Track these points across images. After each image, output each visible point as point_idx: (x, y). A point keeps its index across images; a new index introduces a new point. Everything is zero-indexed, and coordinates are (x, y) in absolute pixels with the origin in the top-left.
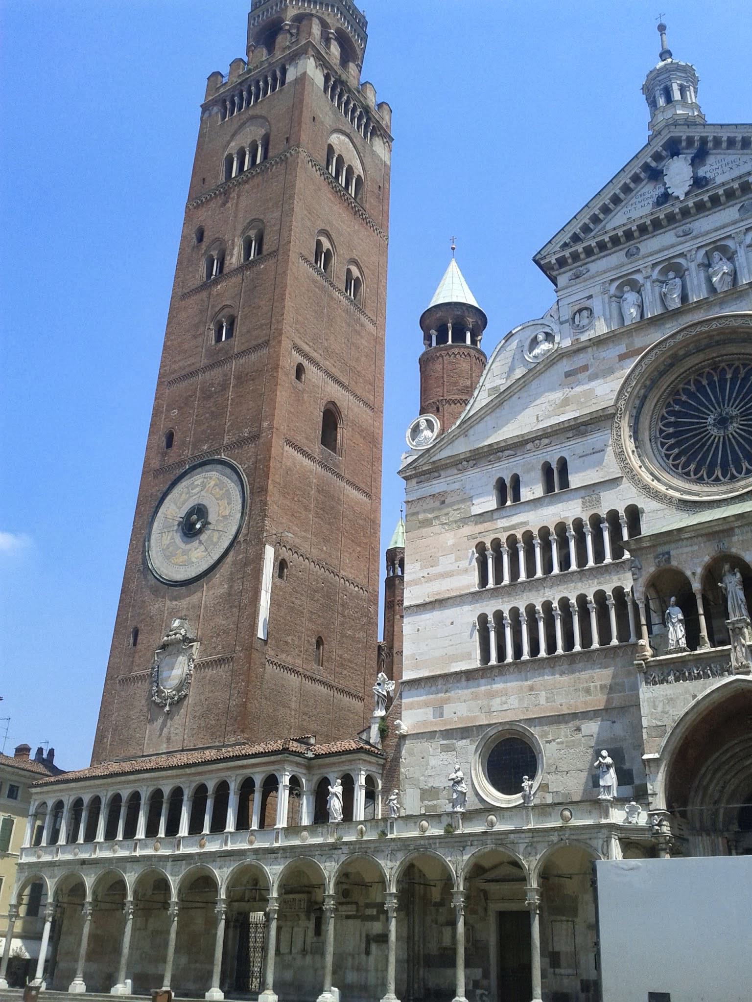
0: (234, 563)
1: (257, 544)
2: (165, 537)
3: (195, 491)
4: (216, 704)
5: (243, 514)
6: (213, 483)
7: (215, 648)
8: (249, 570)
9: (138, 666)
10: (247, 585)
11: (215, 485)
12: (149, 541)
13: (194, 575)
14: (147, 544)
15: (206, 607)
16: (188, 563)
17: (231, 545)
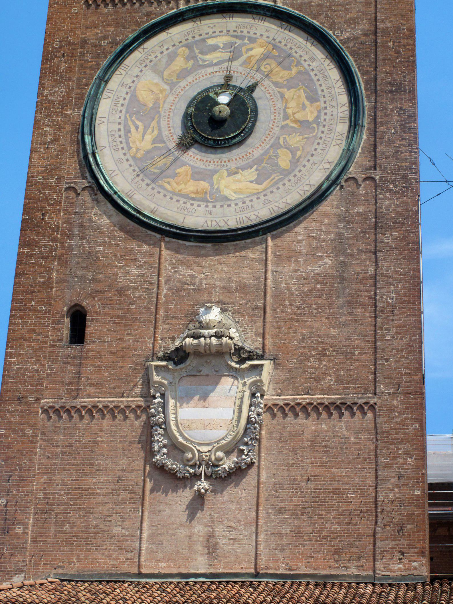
0: (345, 219)
1: (402, 193)
2: (135, 135)
3: (213, 57)
4: (336, 492)
5: (354, 125)
6: (258, 51)
7: (317, 380)
8: (388, 238)
9: (97, 384)
10: (389, 266)
11: (266, 57)
12: (92, 133)
13: (232, 224)
14: (87, 138)
15: (278, 295)
16: (211, 198)
17: (333, 182)
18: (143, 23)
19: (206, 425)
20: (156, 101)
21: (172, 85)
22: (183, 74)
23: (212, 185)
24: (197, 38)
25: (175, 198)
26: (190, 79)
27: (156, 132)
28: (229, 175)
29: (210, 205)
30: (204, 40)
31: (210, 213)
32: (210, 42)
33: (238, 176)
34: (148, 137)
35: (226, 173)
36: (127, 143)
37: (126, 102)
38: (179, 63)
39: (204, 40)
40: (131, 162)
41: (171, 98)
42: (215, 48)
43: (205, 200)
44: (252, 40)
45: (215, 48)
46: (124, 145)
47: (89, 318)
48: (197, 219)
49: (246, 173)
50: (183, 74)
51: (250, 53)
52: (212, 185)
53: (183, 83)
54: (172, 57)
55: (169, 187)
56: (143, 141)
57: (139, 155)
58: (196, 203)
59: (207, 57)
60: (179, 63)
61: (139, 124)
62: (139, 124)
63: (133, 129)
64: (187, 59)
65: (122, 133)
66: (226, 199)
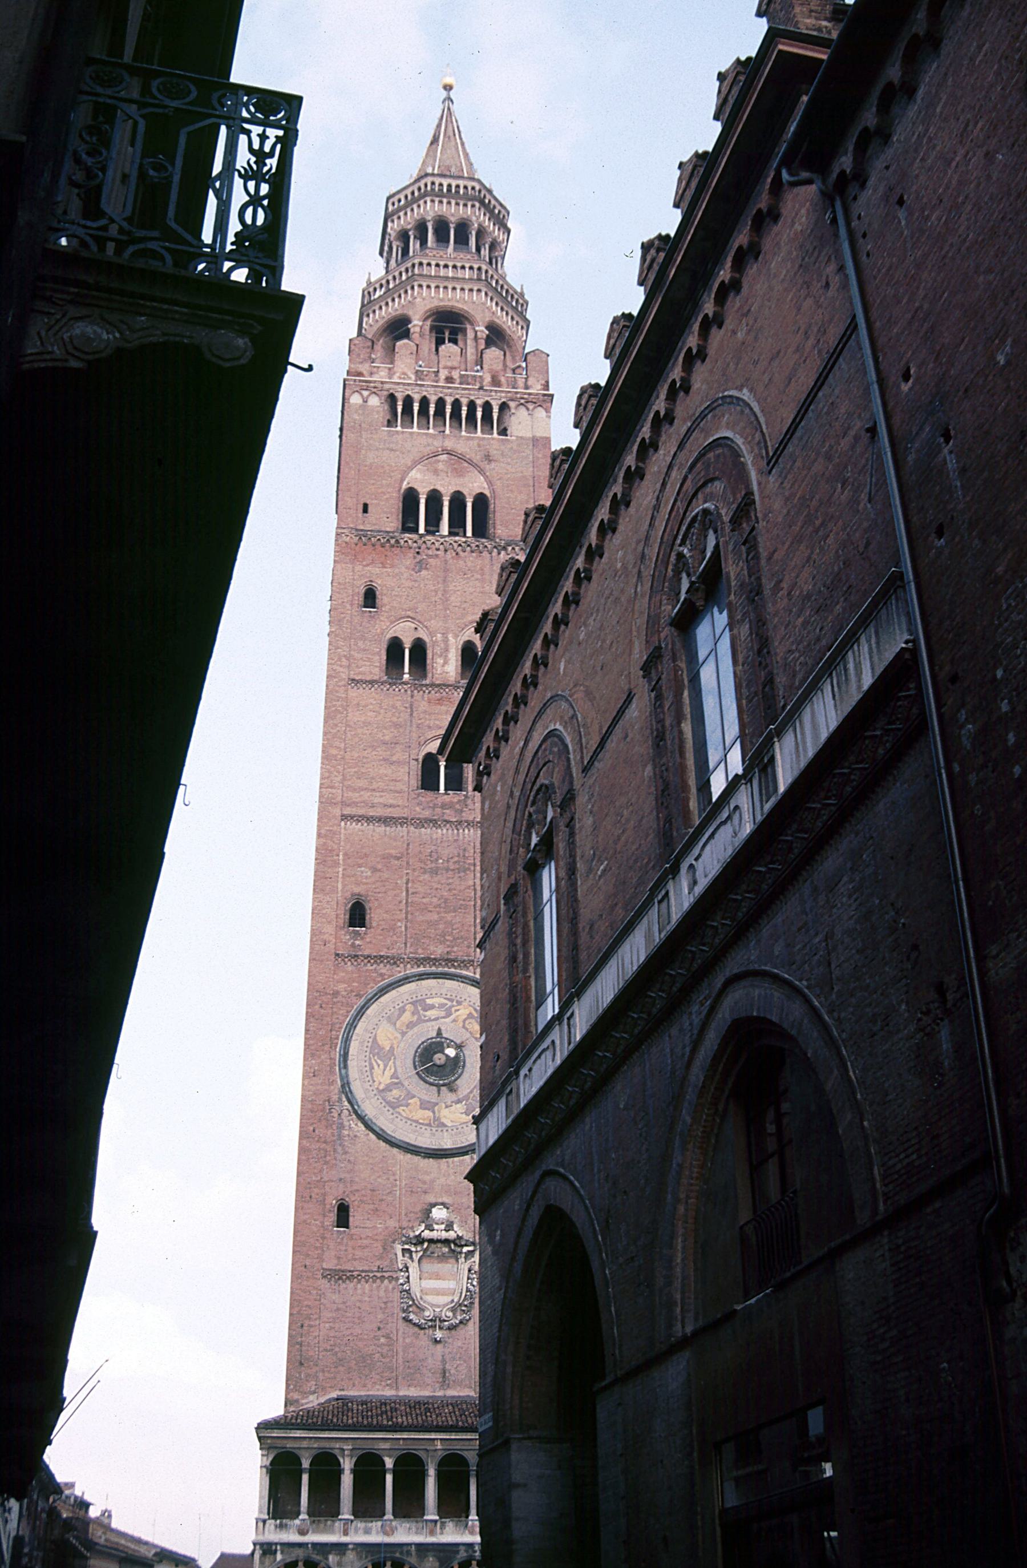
2: (377, 1071)
3: (432, 1013)
18: (379, 982)
19: (438, 1292)
20: (392, 1047)
21: (403, 1034)
22: (411, 1025)
23: (434, 1112)
24: (419, 998)
25: (409, 1122)
26: (415, 1029)
27: (393, 1070)
28: (447, 1107)
29: (434, 1129)
30: (424, 1000)
31: (434, 1135)
32: (429, 1001)
33: (453, 1108)
34: (389, 1073)
35: (444, 1106)
36: (372, 1074)
37: (369, 1045)
38: (407, 1017)
39: (424, 1000)
40: (375, 1092)
41: (402, 1045)
42: (432, 1007)
43: (429, 1125)
44: (459, 1003)
45: (432, 1007)
46: (369, 1078)
47: (351, 1210)
48: (425, 1141)
49: (459, 1106)
50: (411, 1025)
51: (458, 1013)
52: (434, 1112)
53: (410, 1033)
54: (402, 1010)
55: (403, 1114)
56: (383, 1077)
57: (381, 1087)
58: (424, 1127)
59: (428, 1013)
60: (407, 1017)
61: (380, 1062)
62: (380, 1062)
63: (376, 1067)
64: (413, 1014)
65: (368, 1069)
66: (444, 1125)
